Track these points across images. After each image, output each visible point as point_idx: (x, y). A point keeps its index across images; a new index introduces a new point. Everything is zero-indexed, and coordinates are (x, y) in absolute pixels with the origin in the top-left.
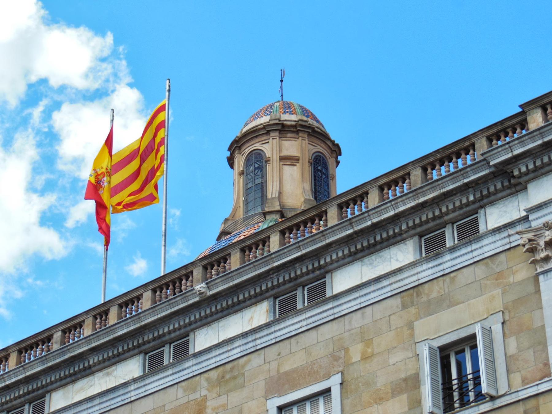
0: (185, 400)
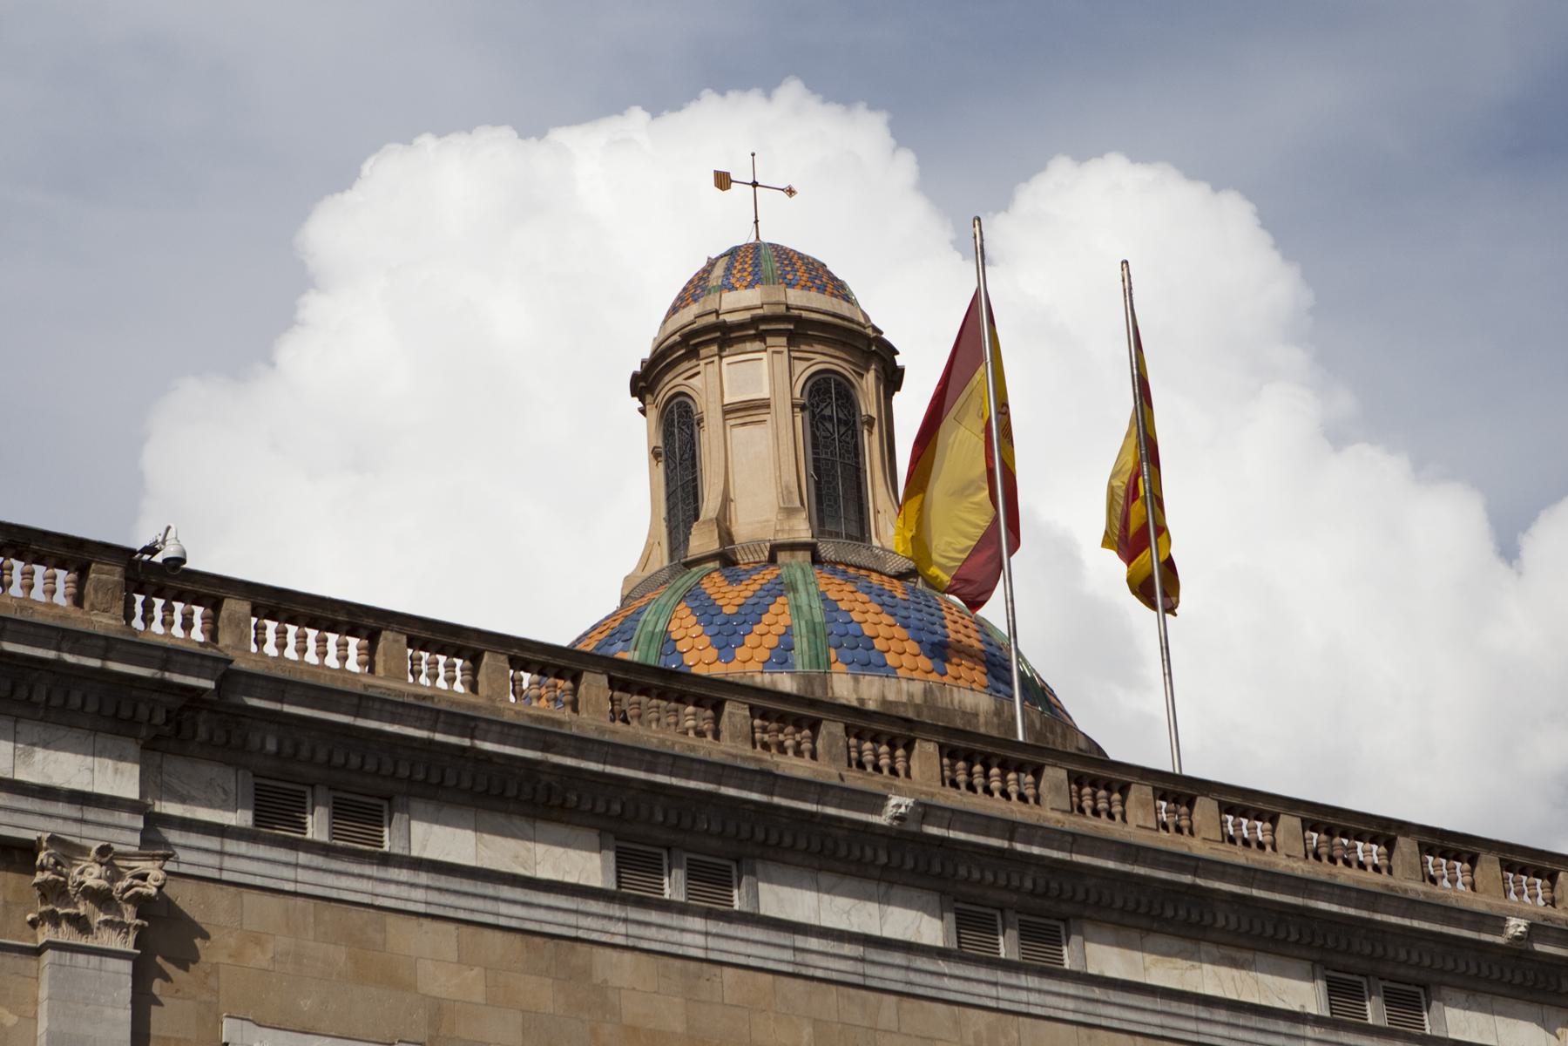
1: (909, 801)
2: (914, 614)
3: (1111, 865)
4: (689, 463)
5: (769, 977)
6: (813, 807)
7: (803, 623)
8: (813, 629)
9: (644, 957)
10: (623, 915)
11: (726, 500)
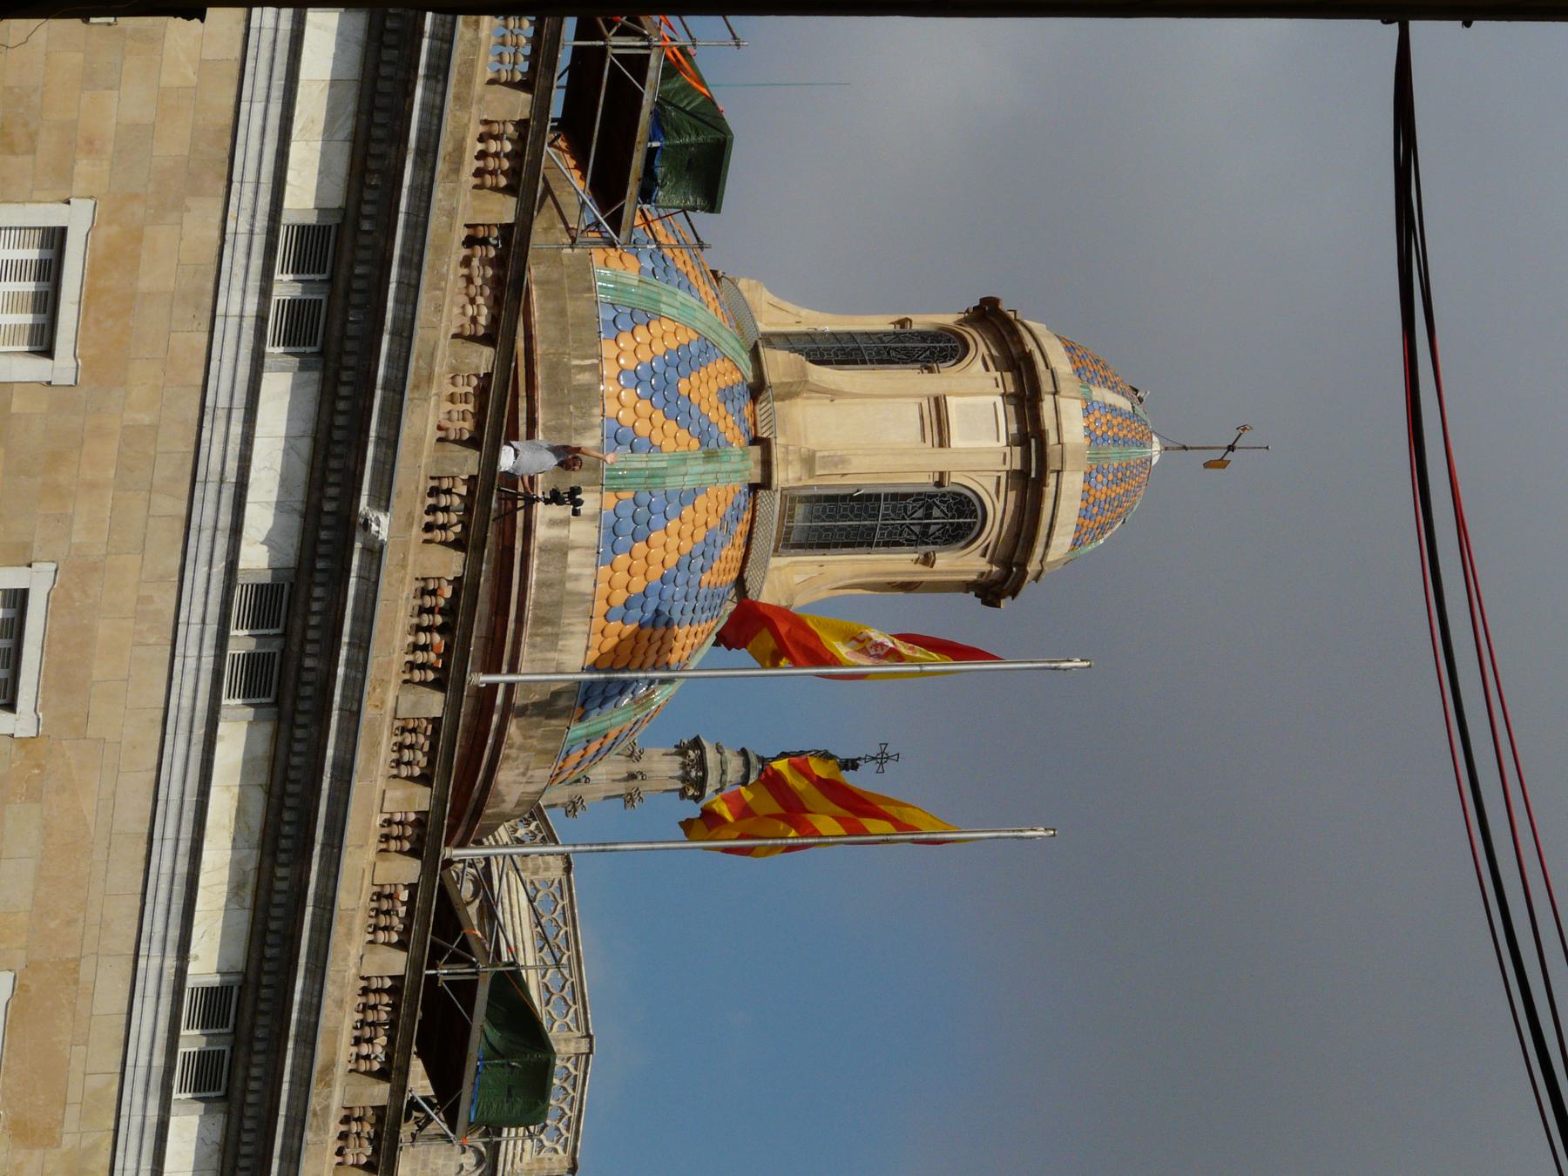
0: (74, 1094)
1: (384, 535)
2: (679, 591)
3: (330, 752)
4: (885, 356)
5: (200, 381)
6: (373, 433)
7: (664, 464)
8: (654, 474)
9: (215, 251)
10: (257, 230)
11: (834, 394)
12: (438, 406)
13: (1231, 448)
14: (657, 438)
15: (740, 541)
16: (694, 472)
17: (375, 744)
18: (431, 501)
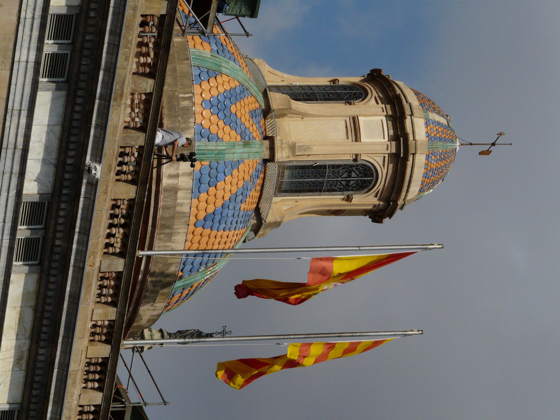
1: (98, 176)
2: (231, 213)
3: (68, 289)
4: (327, 97)
6: (93, 123)
7: (224, 148)
8: (219, 152)
9: (14, 28)
10: (36, 17)
11: (303, 115)
12: (125, 109)
13: (493, 144)
14: (221, 135)
15: (259, 188)
16: (239, 152)
17: (90, 285)
18: (120, 159)
